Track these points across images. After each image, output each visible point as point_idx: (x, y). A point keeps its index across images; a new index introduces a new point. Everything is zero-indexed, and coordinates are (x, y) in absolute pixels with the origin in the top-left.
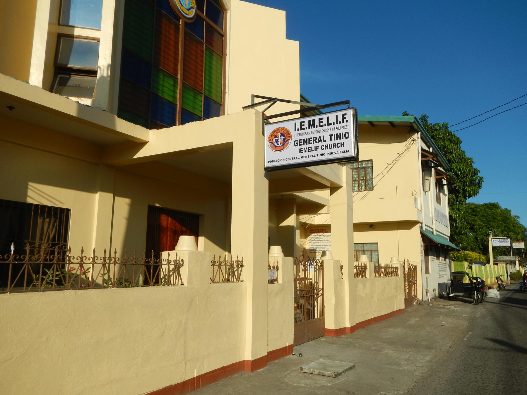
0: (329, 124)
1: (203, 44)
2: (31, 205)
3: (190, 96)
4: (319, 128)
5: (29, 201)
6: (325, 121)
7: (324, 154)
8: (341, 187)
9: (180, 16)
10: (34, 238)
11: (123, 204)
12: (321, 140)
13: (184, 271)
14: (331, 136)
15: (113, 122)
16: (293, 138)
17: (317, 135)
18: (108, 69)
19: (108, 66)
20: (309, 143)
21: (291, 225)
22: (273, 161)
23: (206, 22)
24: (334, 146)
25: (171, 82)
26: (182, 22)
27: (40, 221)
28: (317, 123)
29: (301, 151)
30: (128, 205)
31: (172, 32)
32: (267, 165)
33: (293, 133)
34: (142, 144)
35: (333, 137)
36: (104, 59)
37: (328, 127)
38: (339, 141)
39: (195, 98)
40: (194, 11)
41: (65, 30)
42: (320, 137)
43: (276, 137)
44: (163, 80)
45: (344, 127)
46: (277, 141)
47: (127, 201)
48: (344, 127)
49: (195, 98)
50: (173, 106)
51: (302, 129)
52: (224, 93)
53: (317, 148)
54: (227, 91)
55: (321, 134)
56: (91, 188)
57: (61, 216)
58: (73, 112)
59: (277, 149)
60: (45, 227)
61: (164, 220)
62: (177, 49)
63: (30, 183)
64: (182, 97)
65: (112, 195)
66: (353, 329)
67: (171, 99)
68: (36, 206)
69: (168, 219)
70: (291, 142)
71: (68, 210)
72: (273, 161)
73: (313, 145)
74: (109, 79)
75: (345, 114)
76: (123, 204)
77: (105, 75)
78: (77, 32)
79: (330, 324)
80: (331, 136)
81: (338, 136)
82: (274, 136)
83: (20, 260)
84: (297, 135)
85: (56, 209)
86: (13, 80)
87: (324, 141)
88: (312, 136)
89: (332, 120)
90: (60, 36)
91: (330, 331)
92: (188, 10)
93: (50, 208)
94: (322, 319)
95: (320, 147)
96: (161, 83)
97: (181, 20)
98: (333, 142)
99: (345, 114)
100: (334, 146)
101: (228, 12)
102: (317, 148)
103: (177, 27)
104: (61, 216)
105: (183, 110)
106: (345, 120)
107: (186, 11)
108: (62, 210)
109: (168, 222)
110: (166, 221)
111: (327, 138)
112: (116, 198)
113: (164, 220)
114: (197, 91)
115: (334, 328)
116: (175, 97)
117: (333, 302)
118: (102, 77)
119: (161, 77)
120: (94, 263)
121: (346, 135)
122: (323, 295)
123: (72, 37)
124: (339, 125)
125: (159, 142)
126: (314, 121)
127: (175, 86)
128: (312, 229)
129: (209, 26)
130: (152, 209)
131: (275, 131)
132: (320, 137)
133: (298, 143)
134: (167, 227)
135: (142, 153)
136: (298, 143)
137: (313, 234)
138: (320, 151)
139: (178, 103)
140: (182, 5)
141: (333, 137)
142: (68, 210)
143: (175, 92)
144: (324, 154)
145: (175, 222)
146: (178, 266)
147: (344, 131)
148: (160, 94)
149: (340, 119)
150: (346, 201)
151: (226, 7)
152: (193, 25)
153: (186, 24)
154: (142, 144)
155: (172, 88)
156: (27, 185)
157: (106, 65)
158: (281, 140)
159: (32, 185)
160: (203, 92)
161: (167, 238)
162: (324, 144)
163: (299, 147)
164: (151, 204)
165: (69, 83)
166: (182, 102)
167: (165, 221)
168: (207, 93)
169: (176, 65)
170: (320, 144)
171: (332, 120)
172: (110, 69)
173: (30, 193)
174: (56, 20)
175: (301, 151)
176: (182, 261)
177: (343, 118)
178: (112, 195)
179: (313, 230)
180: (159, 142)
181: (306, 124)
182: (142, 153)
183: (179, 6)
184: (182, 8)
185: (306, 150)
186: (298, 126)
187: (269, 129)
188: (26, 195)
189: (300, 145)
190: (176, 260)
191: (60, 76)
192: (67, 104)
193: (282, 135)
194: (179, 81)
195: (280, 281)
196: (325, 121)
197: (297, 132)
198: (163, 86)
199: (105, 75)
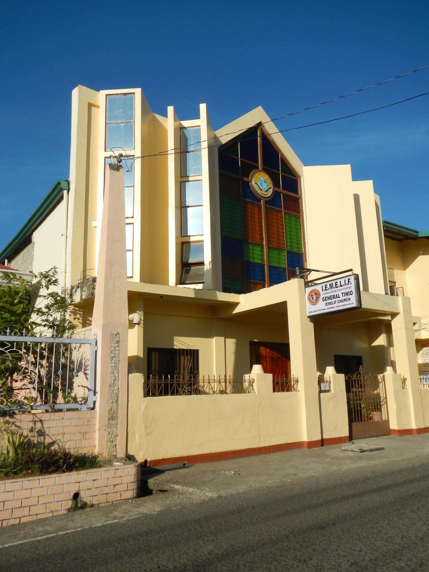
0: (341, 286)
1: (282, 211)
2: (176, 349)
3: (275, 254)
4: (336, 289)
5: (175, 347)
6: (339, 284)
7: (340, 306)
10: (180, 369)
11: (231, 343)
12: (338, 296)
13: (255, 385)
14: (342, 293)
15: (216, 295)
16: (322, 296)
17: (335, 294)
18: (210, 265)
19: (210, 263)
20: (331, 299)
21: (381, 344)
22: (311, 312)
23: (283, 194)
24: (345, 300)
25: (259, 249)
26: (263, 202)
27: (182, 359)
28: (334, 286)
29: (326, 304)
31: (256, 212)
32: (308, 314)
33: (321, 293)
34: (235, 305)
35: (344, 294)
36: (207, 257)
37: (341, 288)
38: (347, 297)
39: (279, 255)
40: (272, 190)
41: (185, 239)
42: (336, 295)
43: (312, 296)
44: (253, 249)
45: (350, 288)
46: (313, 298)
48: (350, 288)
49: (279, 255)
50: (262, 266)
51: (326, 290)
52: (305, 244)
53: (335, 302)
54: (306, 242)
55: (337, 293)
56: (209, 335)
57: (194, 354)
58: (192, 295)
59: (314, 303)
60: (185, 362)
62: (261, 223)
63: (175, 337)
64: (268, 257)
65: (223, 338)
66: (420, 431)
67: (259, 261)
68: (180, 350)
69: (266, 350)
70: (321, 299)
71: (198, 351)
72: (311, 312)
73: (333, 300)
74: (211, 270)
75: (350, 279)
76: (231, 343)
77: (208, 268)
78: (192, 239)
79: (394, 425)
80: (342, 293)
81: (347, 294)
82: (310, 295)
83: (172, 381)
84: (324, 294)
85: (190, 350)
86: (161, 286)
87: (339, 297)
88: (332, 294)
89: (343, 283)
90: (183, 243)
91: (394, 431)
92: (267, 191)
93: (187, 350)
94: (387, 422)
95: (337, 301)
96: (251, 251)
97: (262, 201)
98: (344, 298)
99: (350, 279)
100: (345, 300)
101: (302, 178)
102: (335, 302)
103: (260, 206)
104: (194, 354)
105: (270, 267)
106: (350, 283)
107: (265, 193)
108: (194, 350)
109: (266, 351)
110: (265, 351)
111: (341, 295)
112: (227, 339)
114: (280, 249)
115: (397, 429)
116: (262, 259)
117: (395, 407)
118: (207, 270)
119: (251, 247)
120: (204, 382)
121: (350, 293)
122: (386, 402)
123: (189, 243)
124: (346, 286)
125: (247, 302)
126: (332, 284)
127: (262, 251)
128: (423, 343)
129: (285, 196)
130: (252, 344)
131: (311, 292)
132: (336, 295)
133: (325, 299)
134: (266, 355)
135: (238, 310)
136: (325, 299)
137: (425, 348)
138: (337, 304)
139: (266, 263)
140: (261, 190)
141: (344, 294)
142: (198, 351)
143: (262, 255)
144: (340, 306)
146: (251, 383)
147: (349, 290)
148: (251, 260)
149: (347, 282)
150: (404, 326)
151: (299, 175)
152: (273, 200)
153: (266, 202)
154: (235, 305)
155: (260, 253)
156: (173, 338)
157: (208, 262)
158: (315, 297)
159: (175, 337)
160: (285, 249)
161: (267, 363)
162: (339, 299)
163: (325, 302)
164: (252, 340)
165: (191, 273)
166: (269, 261)
167: (263, 351)
168: (289, 248)
169: (261, 235)
170: (337, 299)
171: (343, 283)
172: (211, 264)
173: (175, 343)
174: (179, 235)
175: (326, 304)
176: (254, 380)
177: (349, 282)
178: (223, 338)
179: (424, 344)
180: (247, 302)
181: (328, 287)
182: (238, 310)
183: (259, 191)
184: (262, 192)
185: (330, 303)
186: (324, 288)
187: (309, 290)
188: (173, 345)
189: (326, 300)
190: (250, 380)
191: (185, 268)
192: (189, 290)
193: (316, 294)
194: (265, 247)
195: (332, 391)
196: (339, 284)
197: (324, 292)
198: (253, 253)
199: (208, 268)
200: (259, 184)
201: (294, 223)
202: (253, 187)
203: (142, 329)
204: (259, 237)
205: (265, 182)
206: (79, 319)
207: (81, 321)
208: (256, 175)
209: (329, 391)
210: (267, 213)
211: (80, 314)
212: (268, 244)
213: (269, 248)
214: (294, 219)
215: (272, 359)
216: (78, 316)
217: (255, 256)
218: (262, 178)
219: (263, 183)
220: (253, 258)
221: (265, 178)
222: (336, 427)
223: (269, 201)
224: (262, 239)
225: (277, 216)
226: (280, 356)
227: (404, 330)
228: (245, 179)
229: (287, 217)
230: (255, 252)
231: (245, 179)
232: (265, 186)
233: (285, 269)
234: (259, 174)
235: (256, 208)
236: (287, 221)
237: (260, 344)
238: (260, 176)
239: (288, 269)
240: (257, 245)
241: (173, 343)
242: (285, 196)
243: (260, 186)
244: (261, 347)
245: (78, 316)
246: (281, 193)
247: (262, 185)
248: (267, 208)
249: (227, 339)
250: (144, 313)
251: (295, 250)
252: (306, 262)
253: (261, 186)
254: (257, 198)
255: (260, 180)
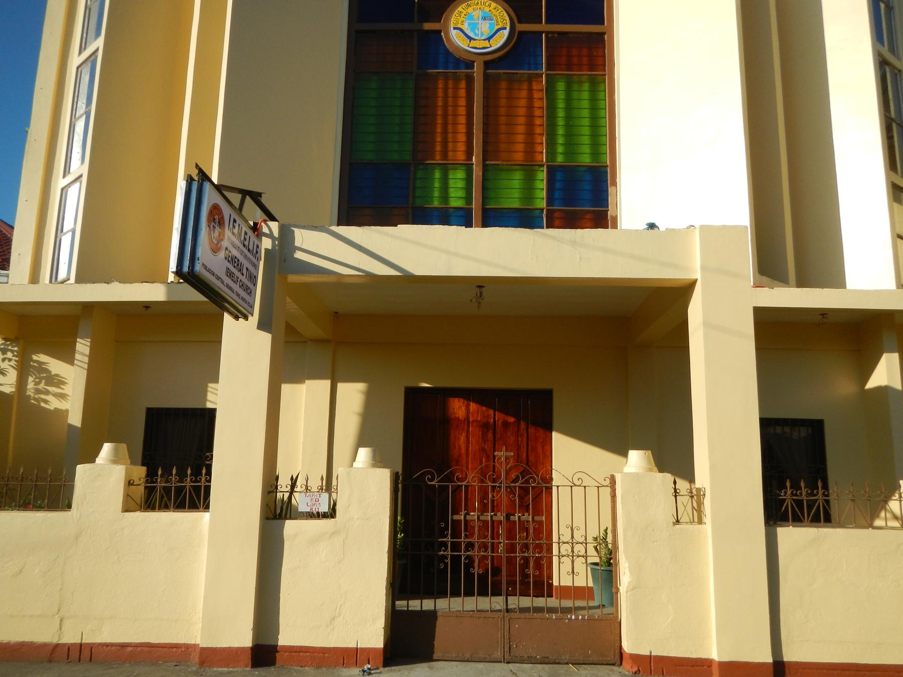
8: (693, 283)
9: (472, 58)
11: (352, 395)
25: (460, 174)
30: (362, 392)
31: (462, 93)
40: (506, 33)
47: (361, 386)
61: (460, 407)
63: (210, 385)
65: (327, 384)
76: (352, 395)
92: (489, 39)
103: (470, 79)
107: (486, 44)
110: (463, 408)
112: (341, 386)
113: (460, 407)
119: (437, 175)
130: (413, 396)
134: (468, 418)
140: (470, 39)
145: (484, 408)
153: (487, 65)
156: (207, 386)
164: (412, 384)
166: (485, 199)
168: (560, 159)
178: (327, 384)
184: (473, 44)
188: (205, 399)
200: (465, 27)
201: (586, 95)
202: (449, 39)
203: (85, 372)
204: (462, 147)
205: (484, 19)
206: (10, 360)
207: (13, 363)
208: (460, 9)
209: (331, 514)
210: (486, 88)
211: (12, 351)
212: (484, 160)
213: (485, 168)
214: (586, 86)
215: (485, 426)
216: (9, 355)
217: (453, 193)
218: (477, 14)
219: (480, 22)
220: (445, 197)
221: (487, 9)
222: (333, 619)
223: (500, 59)
224: (469, 153)
225: (530, 90)
226: (512, 420)
227: (702, 330)
228: (428, 26)
229: (561, 86)
230: (452, 183)
231: (428, 26)
232: (486, 28)
233: (542, 210)
234: (469, 6)
235: (463, 84)
236: (561, 95)
237: (443, 394)
238: (470, 10)
239: (547, 210)
240: (456, 165)
241: (206, 396)
242: (555, 40)
243: (467, 32)
244: (451, 399)
245: (9, 355)
246: (542, 32)
247: (474, 26)
248: (486, 78)
249: (341, 386)
250: (91, 342)
251: (586, 159)
252: (614, 184)
253: (473, 30)
254: (464, 62)
255: (472, 18)
